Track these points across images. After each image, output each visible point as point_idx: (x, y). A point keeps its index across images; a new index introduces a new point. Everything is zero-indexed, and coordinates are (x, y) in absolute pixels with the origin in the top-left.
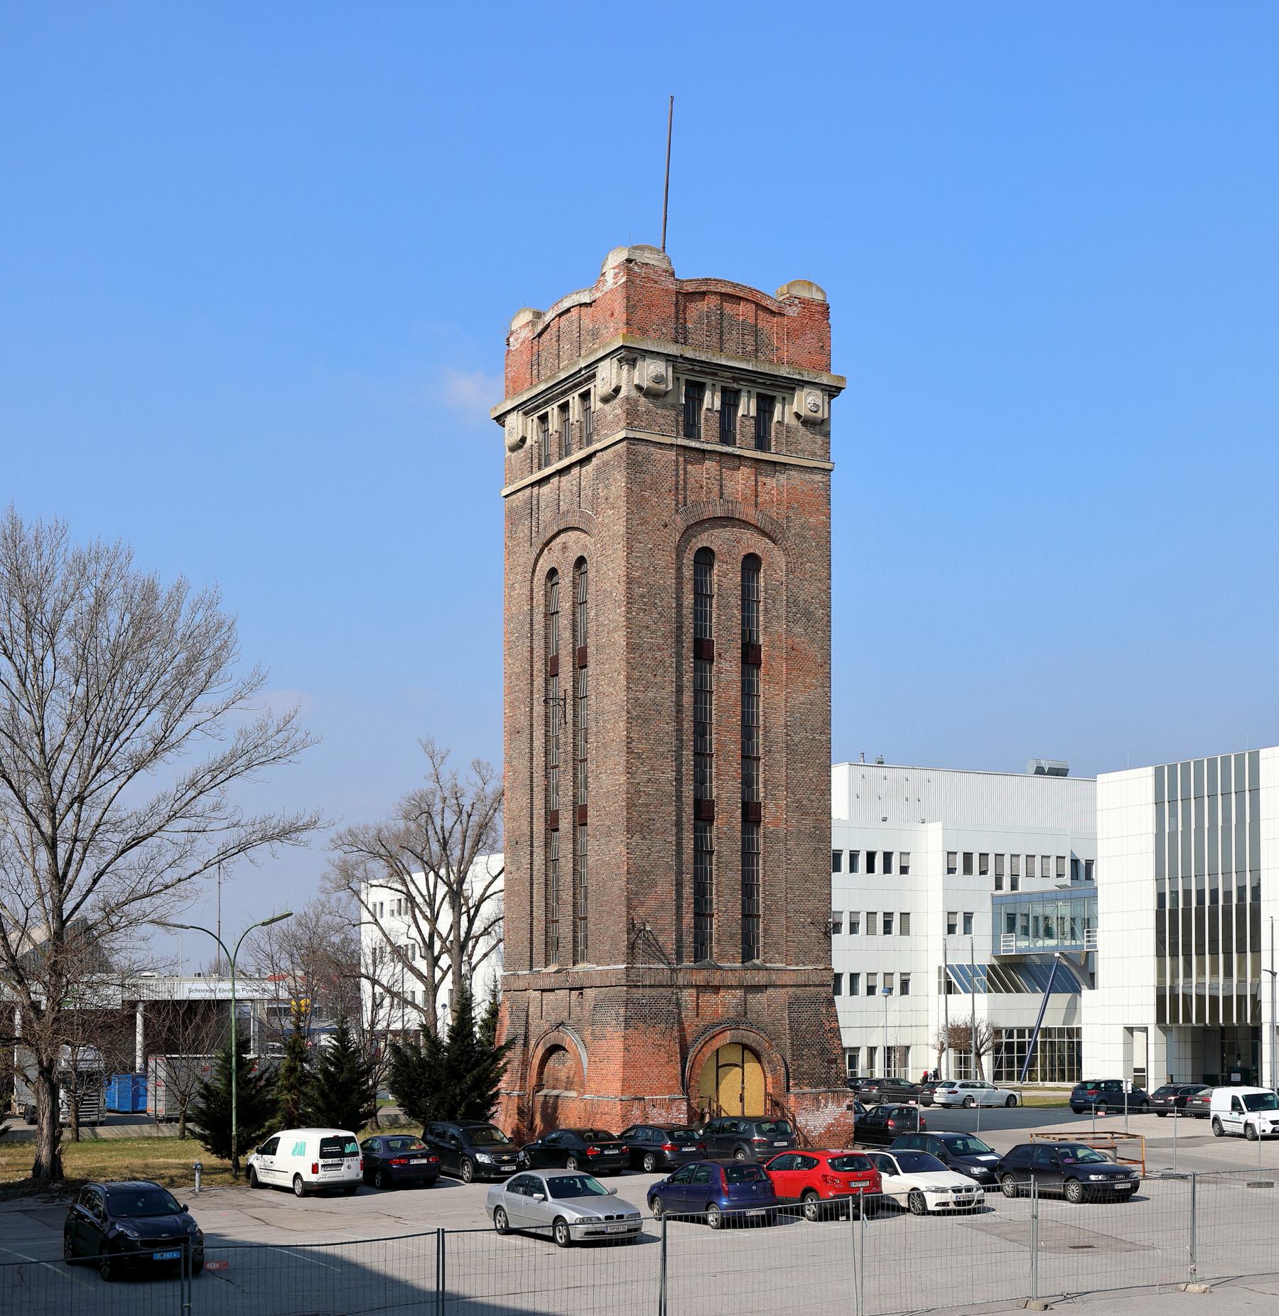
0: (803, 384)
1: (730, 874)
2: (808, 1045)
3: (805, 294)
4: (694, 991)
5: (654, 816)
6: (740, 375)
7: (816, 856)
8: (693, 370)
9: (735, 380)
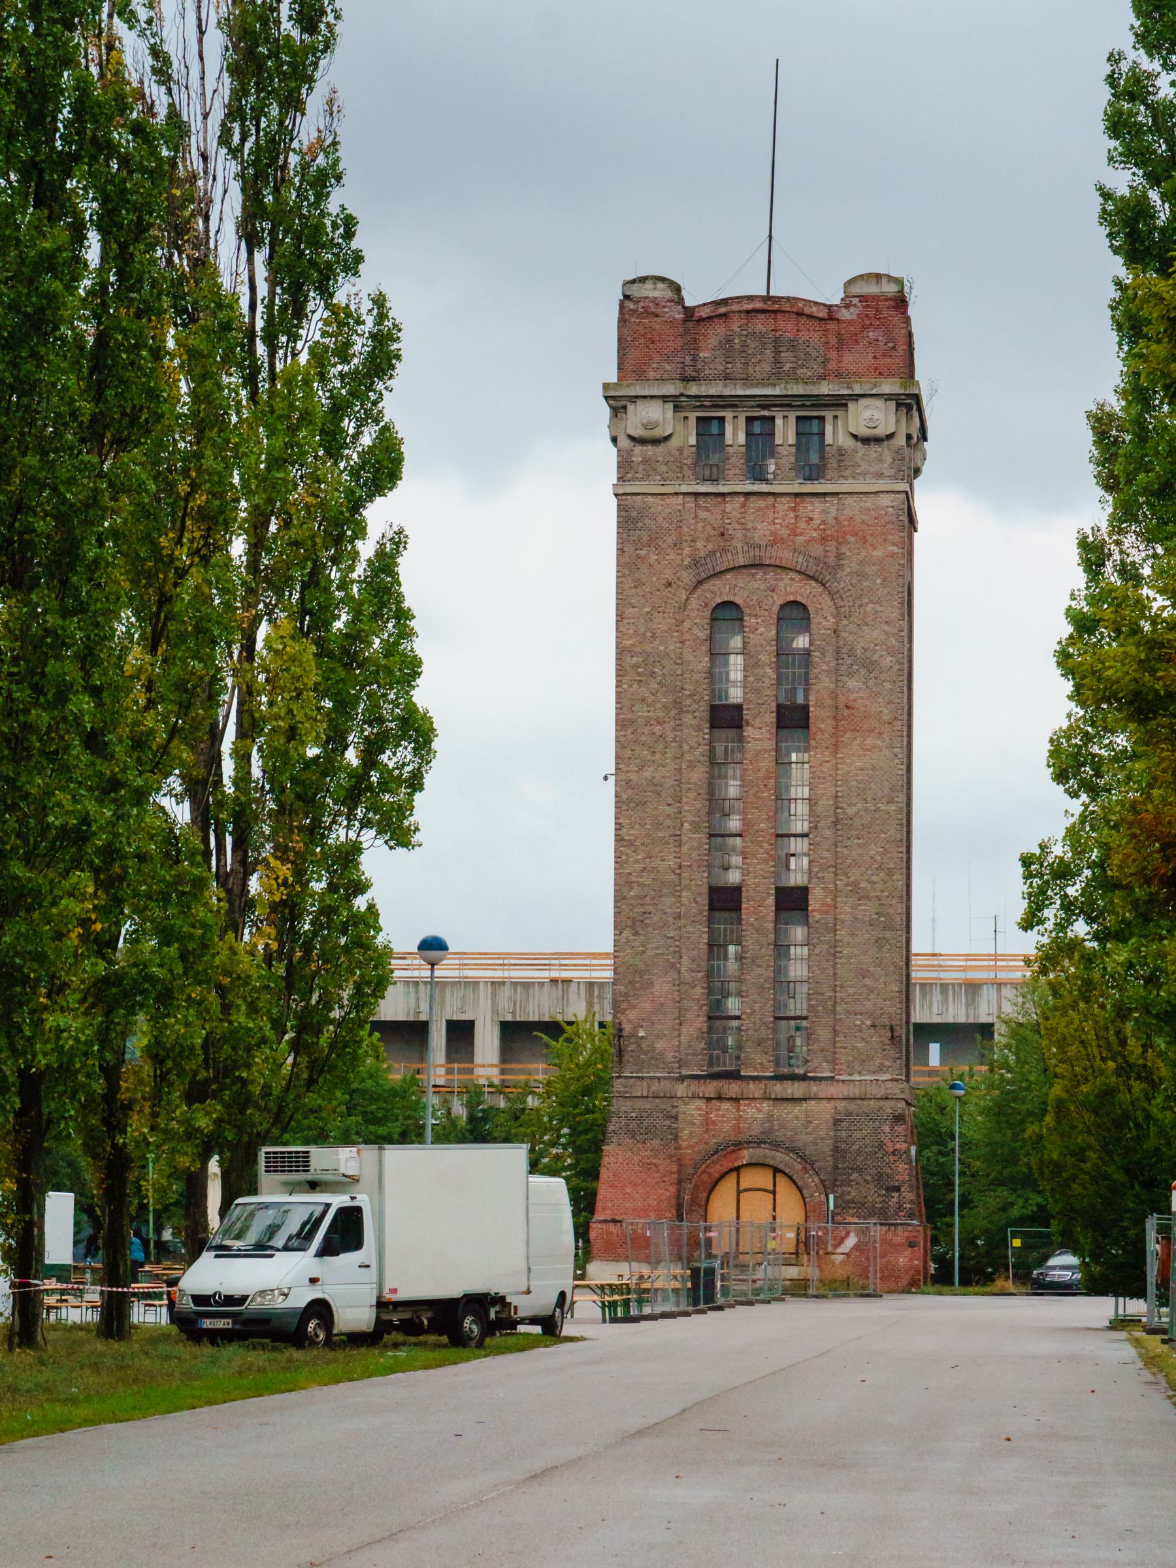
0: (857, 397)
1: (759, 971)
2: (859, 1170)
3: (872, 289)
4: (701, 1103)
5: (650, 908)
6: (767, 402)
7: (880, 947)
8: (702, 406)
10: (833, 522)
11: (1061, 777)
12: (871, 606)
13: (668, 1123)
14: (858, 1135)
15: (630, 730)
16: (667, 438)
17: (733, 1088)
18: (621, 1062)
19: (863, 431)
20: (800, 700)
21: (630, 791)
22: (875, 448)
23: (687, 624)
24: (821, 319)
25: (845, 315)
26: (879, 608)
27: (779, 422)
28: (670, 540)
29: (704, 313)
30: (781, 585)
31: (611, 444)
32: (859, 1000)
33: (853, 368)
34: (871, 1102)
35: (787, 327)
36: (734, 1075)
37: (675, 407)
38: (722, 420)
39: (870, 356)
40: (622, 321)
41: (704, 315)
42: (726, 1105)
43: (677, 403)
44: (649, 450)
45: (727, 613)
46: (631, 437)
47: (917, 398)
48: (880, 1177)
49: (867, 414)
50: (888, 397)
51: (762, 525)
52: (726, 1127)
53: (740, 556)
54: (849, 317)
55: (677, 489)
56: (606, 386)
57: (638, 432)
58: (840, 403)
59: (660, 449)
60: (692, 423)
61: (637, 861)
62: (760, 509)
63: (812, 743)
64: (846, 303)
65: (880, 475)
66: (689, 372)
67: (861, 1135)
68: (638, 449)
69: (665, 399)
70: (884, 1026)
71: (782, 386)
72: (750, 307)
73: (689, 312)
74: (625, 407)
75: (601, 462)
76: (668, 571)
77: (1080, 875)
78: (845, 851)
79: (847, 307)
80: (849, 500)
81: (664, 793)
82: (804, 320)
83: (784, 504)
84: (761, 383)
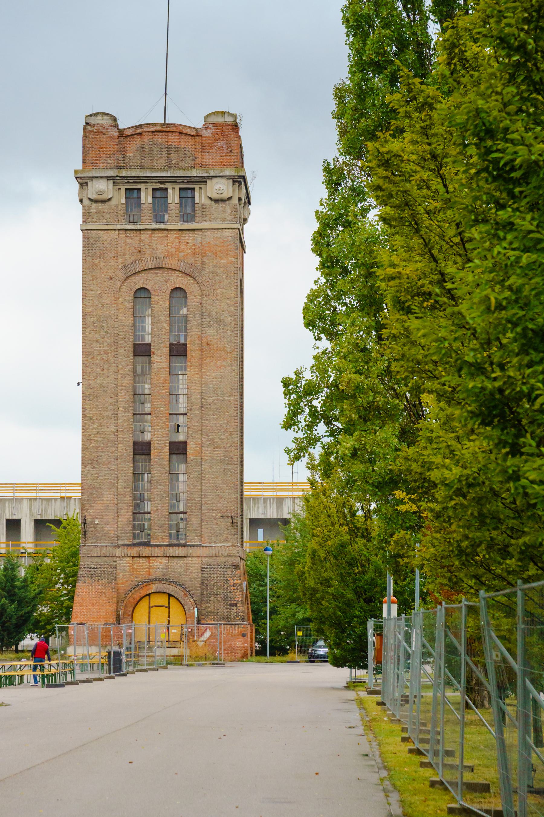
1: (160, 487)
2: (216, 595)
3: (219, 120)
4: (129, 559)
6: (163, 180)
8: (128, 182)
9: (161, 183)
10: (200, 245)
11: (310, 324)
12: (220, 290)
13: (111, 570)
14: (215, 575)
15: (90, 358)
16: (109, 200)
17: (146, 551)
18: (85, 537)
19: (215, 196)
20: (182, 341)
21: (90, 390)
22: (221, 205)
23: (121, 300)
24: (192, 136)
25: (205, 133)
26: (224, 290)
27: (170, 191)
28: (111, 255)
29: (129, 132)
30: (172, 278)
31: (79, 203)
32: (214, 502)
33: (210, 162)
34: (221, 558)
35: (174, 139)
36: (147, 544)
37: (114, 183)
38: (139, 190)
39: (219, 155)
40: (85, 136)
41: (129, 134)
42: (142, 560)
43: (114, 180)
44: (100, 206)
45: (142, 294)
46: (90, 199)
47: (244, 177)
48: (226, 598)
49: (217, 187)
50: (228, 177)
51: (161, 247)
52: (143, 572)
53: (149, 263)
54: (207, 135)
55: (115, 227)
56: (76, 172)
57: (94, 196)
58: (203, 180)
59: (105, 206)
60: (123, 191)
61: (94, 428)
62: (160, 238)
63: (189, 364)
64: (206, 127)
65: (224, 220)
66: (121, 164)
67: (216, 575)
68: (94, 205)
69: (108, 178)
70: (228, 517)
71: (172, 171)
72: (154, 129)
73: (121, 132)
74: (86, 183)
75: (75, 213)
76: (110, 271)
77: (322, 392)
78: (207, 422)
79: (206, 129)
80: (208, 233)
81: (108, 391)
82: (183, 136)
83: (173, 235)
84: (162, 169)
